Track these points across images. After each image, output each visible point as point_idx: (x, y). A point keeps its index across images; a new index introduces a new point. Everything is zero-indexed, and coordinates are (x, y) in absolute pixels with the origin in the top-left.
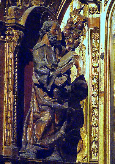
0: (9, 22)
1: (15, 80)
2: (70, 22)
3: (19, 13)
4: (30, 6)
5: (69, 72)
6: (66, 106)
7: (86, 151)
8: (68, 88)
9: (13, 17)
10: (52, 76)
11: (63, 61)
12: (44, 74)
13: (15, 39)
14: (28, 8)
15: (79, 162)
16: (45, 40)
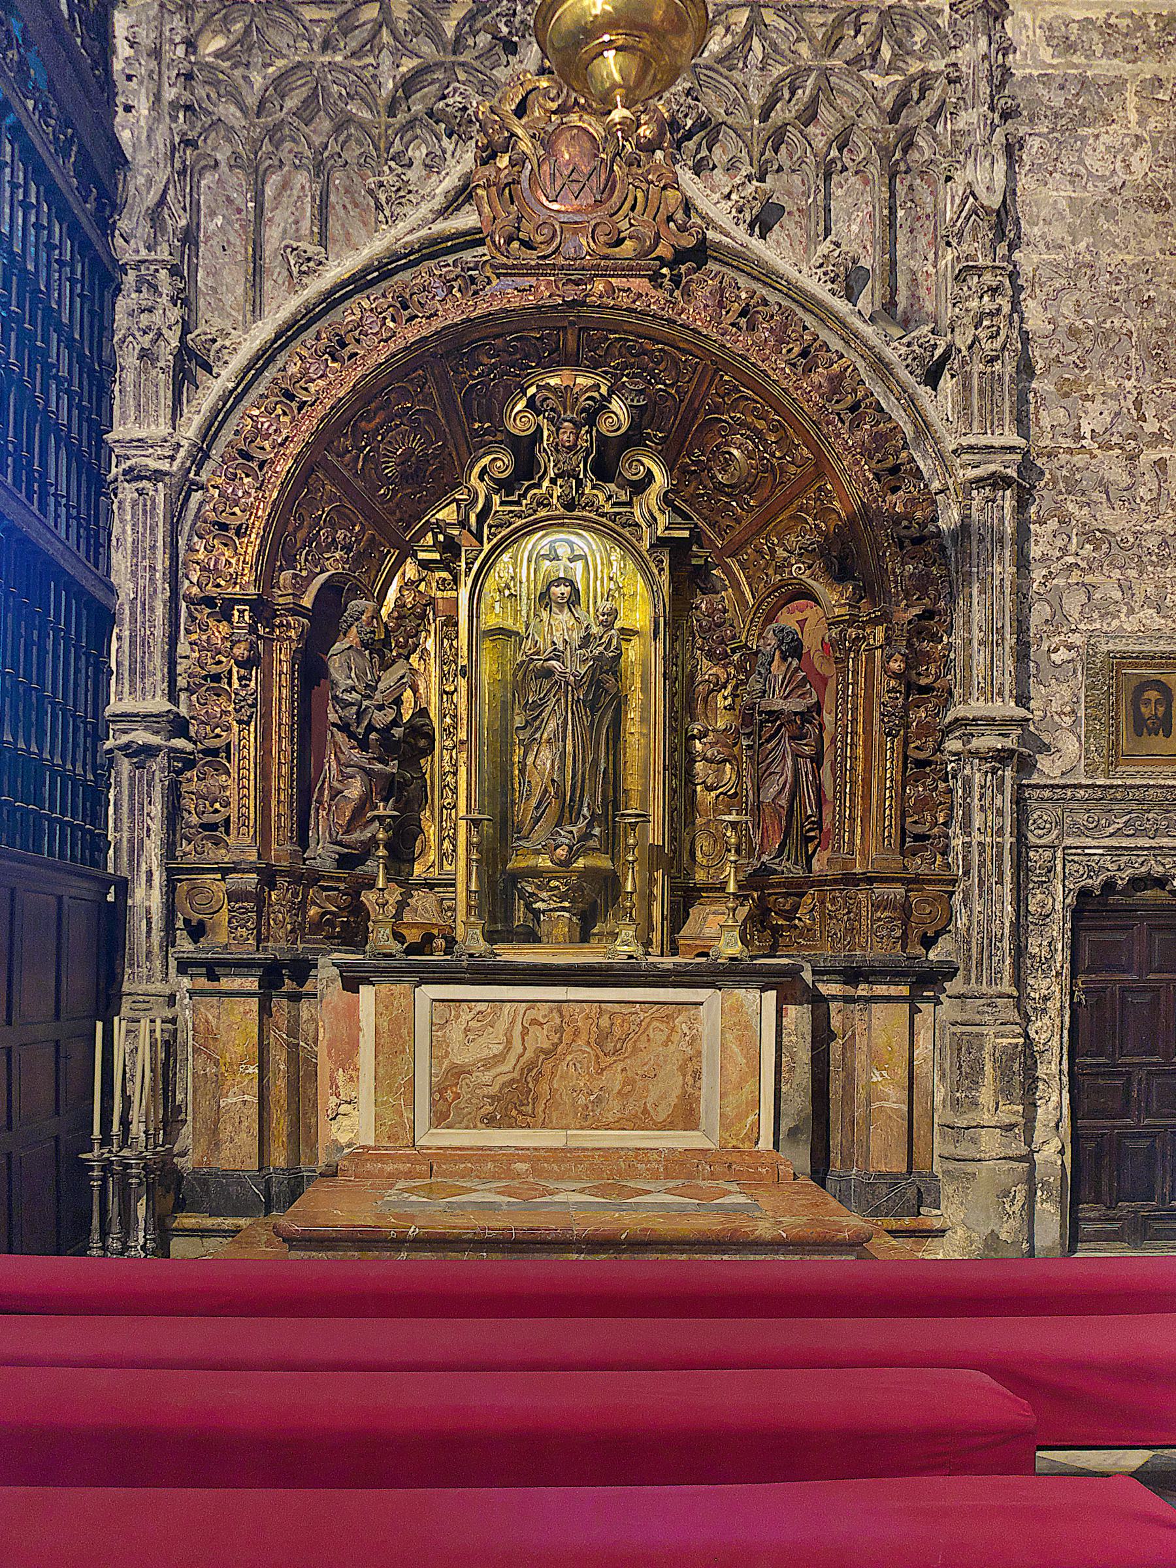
0: (281, 600)
1: (293, 716)
2: (399, 605)
3: (301, 585)
4: (322, 572)
5: (398, 702)
6: (392, 767)
7: (432, 856)
8: (398, 732)
9: (290, 591)
10: (367, 707)
11: (388, 679)
12: (352, 704)
13: (292, 633)
14: (318, 574)
15: (419, 876)
16: (353, 638)
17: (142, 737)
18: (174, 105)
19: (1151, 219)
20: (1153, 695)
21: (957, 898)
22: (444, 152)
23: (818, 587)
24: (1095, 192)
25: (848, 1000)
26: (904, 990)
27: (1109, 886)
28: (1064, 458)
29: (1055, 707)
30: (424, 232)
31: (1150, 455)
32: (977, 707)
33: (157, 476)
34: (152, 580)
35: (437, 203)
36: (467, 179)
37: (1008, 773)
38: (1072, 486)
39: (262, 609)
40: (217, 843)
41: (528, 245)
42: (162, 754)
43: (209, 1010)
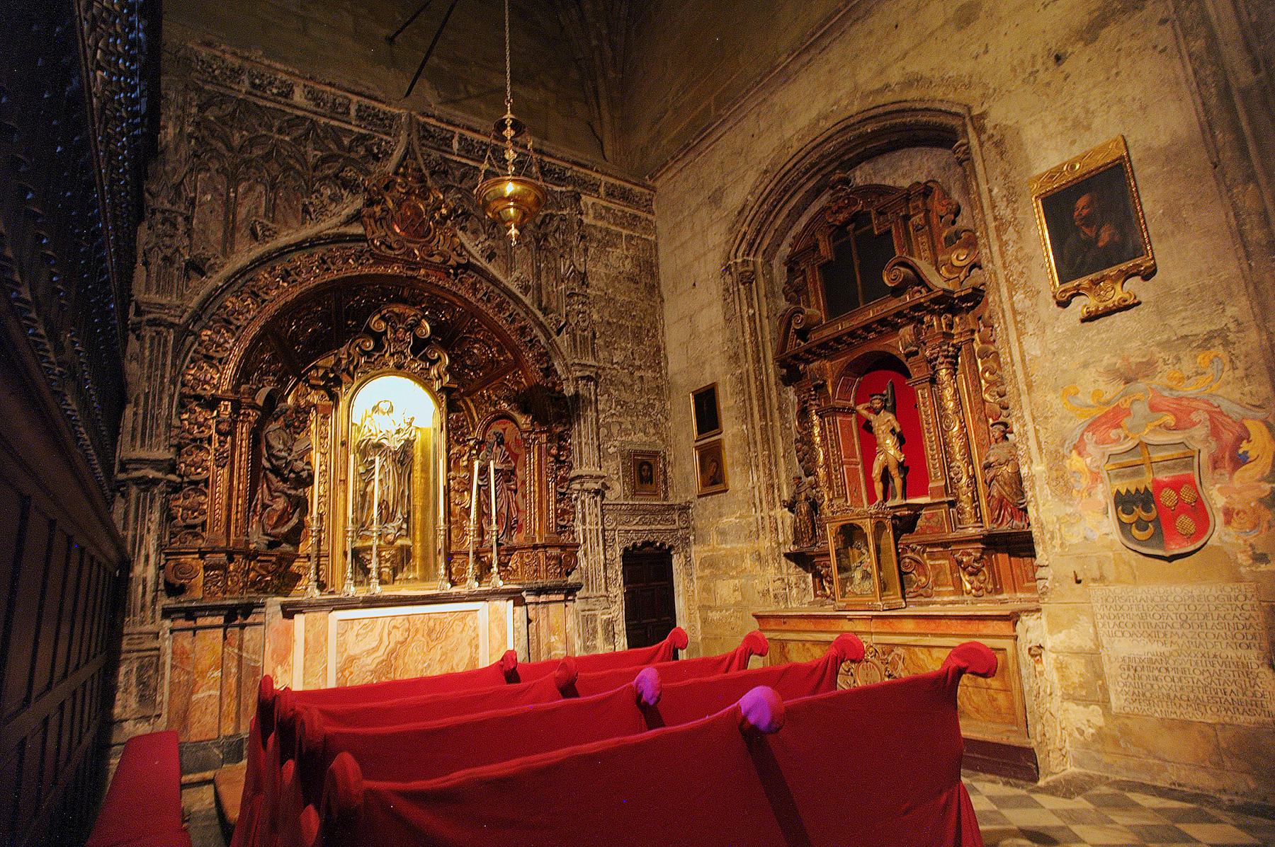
13: (251, 418)
17: (152, 474)
18: (190, 136)
19: (633, 286)
20: (646, 467)
21: (580, 554)
22: (342, 195)
23: (516, 415)
24: (614, 273)
25: (537, 603)
26: (562, 597)
27: (634, 545)
28: (608, 371)
29: (611, 471)
30: (335, 231)
31: (637, 374)
32: (585, 470)
33: (172, 325)
34: (162, 383)
35: (343, 218)
36: (359, 212)
37: (598, 498)
38: (612, 382)
39: (237, 406)
40: (196, 535)
41: (390, 247)
42: (162, 484)
43: (185, 640)
